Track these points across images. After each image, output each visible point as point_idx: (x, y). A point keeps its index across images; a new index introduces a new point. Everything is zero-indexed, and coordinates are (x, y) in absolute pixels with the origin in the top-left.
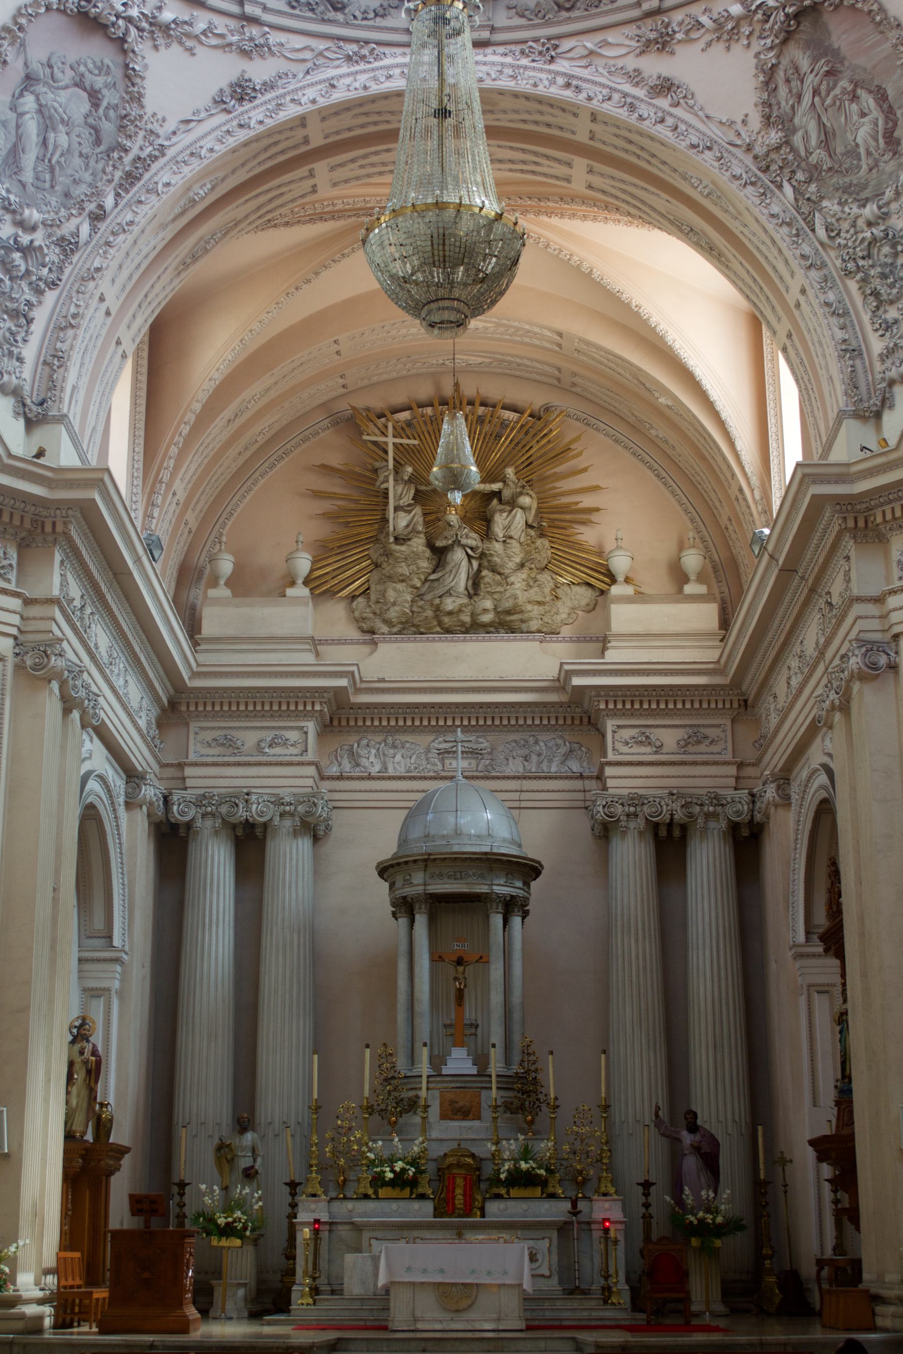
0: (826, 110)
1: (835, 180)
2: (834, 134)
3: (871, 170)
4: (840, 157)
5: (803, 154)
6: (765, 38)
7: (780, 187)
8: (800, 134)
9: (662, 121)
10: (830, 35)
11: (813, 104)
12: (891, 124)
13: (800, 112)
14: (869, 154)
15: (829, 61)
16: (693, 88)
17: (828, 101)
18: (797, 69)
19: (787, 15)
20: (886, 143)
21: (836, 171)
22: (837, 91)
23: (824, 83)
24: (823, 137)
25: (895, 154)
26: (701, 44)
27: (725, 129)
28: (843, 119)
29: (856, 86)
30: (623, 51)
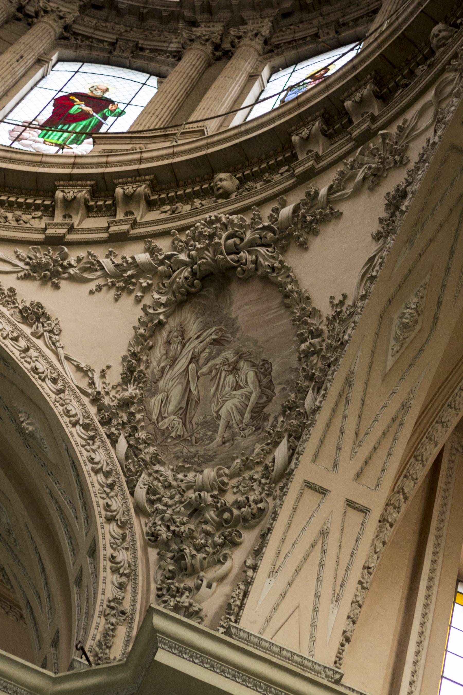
0: (198, 378)
1: (179, 448)
2: (197, 403)
3: (224, 443)
4: (195, 426)
5: (154, 417)
6: (161, 293)
7: (114, 442)
8: (160, 397)
9: (15, 339)
10: (231, 304)
11: (187, 369)
12: (265, 398)
13: (169, 375)
14: (228, 426)
15: (220, 330)
16: (62, 326)
17: (205, 369)
18: (183, 333)
19: (193, 273)
20: (252, 418)
21: (185, 440)
22: (218, 361)
23: (207, 350)
24: (184, 405)
25: (257, 429)
26: (92, 286)
27: (80, 374)
28: (213, 390)
29: (240, 358)
30: (8, 268)
